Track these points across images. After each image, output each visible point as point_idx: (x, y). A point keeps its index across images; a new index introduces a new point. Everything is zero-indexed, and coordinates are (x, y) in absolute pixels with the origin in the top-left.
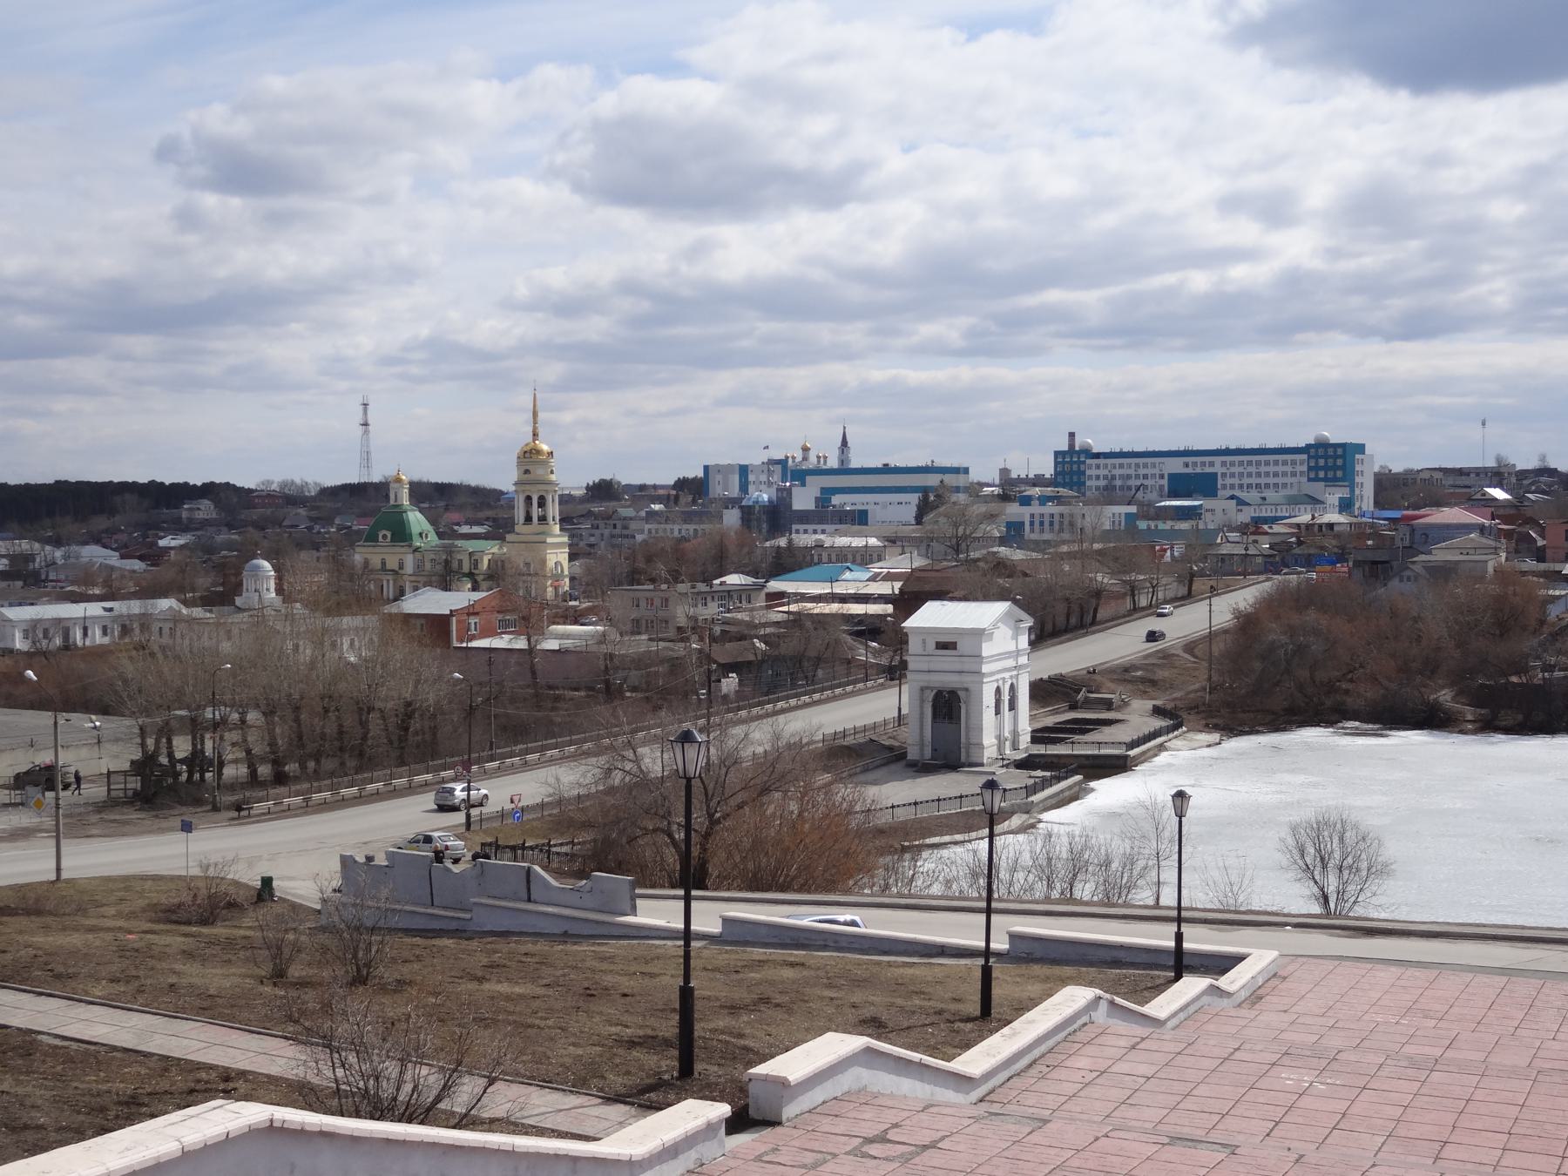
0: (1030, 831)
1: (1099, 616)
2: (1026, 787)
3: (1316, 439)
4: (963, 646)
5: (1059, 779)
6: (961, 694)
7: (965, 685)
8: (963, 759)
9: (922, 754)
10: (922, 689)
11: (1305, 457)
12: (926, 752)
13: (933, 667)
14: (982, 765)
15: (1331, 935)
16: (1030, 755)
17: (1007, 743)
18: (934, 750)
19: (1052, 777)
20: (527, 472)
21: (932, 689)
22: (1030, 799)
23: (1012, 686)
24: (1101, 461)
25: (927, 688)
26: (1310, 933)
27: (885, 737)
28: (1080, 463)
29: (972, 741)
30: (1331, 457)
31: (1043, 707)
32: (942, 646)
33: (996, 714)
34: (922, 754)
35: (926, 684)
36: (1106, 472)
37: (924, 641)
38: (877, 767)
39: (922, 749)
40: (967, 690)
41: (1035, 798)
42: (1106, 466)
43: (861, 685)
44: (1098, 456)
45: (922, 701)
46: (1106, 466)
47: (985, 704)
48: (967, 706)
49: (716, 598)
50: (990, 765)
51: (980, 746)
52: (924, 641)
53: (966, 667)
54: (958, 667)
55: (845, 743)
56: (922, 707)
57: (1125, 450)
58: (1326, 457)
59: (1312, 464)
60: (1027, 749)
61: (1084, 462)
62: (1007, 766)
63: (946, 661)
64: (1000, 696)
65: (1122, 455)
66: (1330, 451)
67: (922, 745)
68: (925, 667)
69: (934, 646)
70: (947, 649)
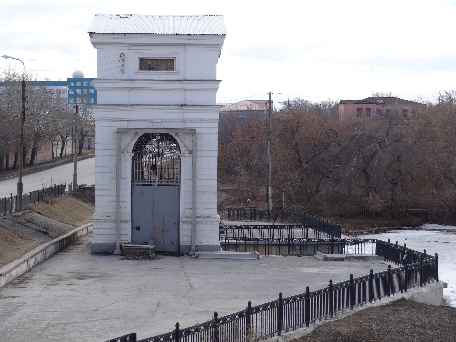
1: (39, 158)
3: (74, 75)
7: (189, 125)
11: (66, 88)
12: (123, 232)
13: (136, 98)
18: (136, 228)
25: (129, 130)
30: (85, 88)
35: (124, 125)
37: (122, 57)
39: (118, 229)
40: (193, 131)
45: (120, 152)
52: (122, 57)
56: (119, 161)
58: (82, 88)
59: (72, 93)
66: (85, 84)
69: (137, 65)
70: (157, 69)
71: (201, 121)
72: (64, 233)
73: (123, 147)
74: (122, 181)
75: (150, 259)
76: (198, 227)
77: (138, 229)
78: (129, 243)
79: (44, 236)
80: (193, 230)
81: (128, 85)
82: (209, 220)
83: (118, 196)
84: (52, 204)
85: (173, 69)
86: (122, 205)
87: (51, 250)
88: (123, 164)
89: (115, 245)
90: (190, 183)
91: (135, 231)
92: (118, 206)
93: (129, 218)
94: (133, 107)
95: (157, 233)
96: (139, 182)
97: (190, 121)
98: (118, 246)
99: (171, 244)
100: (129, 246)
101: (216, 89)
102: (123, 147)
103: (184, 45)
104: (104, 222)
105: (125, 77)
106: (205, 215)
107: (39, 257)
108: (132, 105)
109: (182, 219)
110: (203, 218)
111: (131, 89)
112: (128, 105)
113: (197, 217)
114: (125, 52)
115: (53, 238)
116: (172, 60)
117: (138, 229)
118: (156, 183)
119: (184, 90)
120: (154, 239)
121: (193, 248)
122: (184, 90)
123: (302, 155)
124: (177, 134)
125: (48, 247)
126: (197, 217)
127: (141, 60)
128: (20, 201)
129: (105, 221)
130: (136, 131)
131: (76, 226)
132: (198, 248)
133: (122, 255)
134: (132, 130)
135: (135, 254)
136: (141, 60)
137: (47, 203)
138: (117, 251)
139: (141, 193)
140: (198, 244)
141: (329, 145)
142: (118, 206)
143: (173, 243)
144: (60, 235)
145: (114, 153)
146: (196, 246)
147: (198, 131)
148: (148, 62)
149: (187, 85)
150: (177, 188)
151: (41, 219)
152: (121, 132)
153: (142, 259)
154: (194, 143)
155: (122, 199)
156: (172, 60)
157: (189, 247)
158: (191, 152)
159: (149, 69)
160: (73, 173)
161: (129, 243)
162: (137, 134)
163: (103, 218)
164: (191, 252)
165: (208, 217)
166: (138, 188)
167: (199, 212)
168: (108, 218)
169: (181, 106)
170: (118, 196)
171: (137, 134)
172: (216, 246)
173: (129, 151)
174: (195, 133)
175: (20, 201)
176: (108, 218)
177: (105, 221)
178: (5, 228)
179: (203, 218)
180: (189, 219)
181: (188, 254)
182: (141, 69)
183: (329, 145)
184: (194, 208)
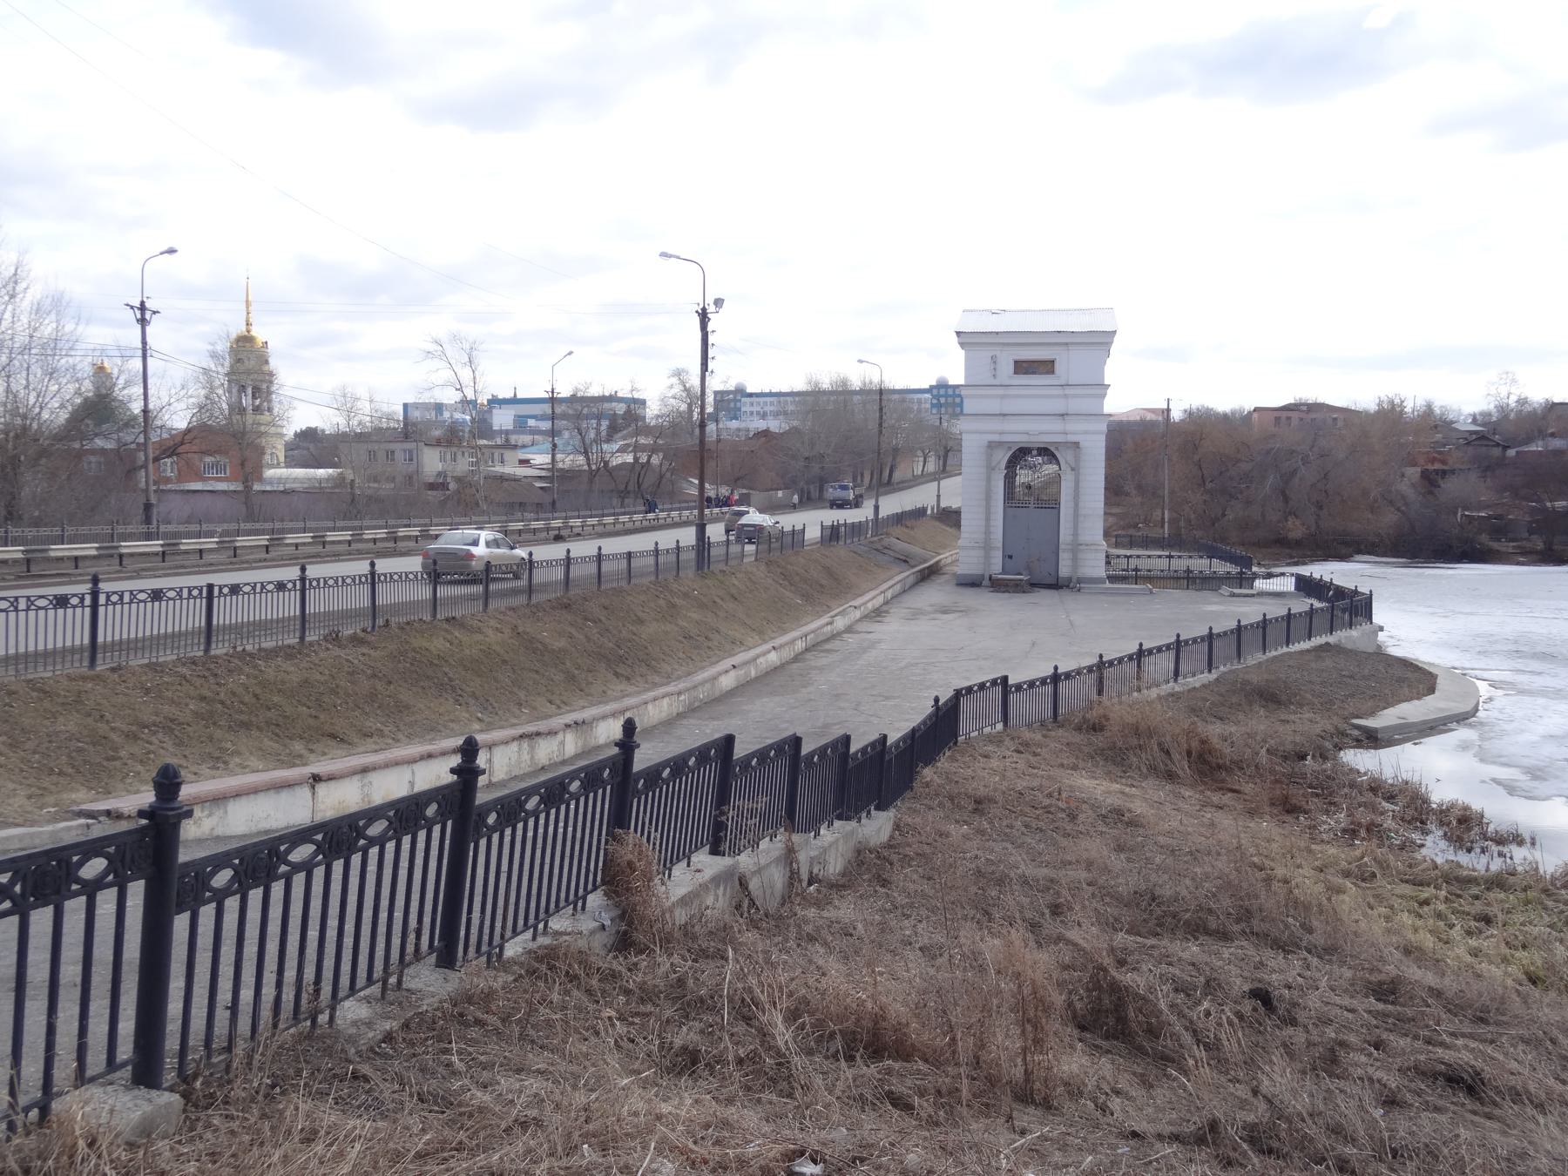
1: (897, 476)
4: (1070, 366)
7: (1071, 438)
11: (928, 396)
20: (239, 360)
24: (754, 399)
25: (1000, 444)
28: (735, 400)
30: (950, 396)
32: (1022, 367)
35: (996, 438)
36: (759, 409)
37: (994, 360)
39: (987, 557)
40: (1076, 445)
42: (759, 403)
44: (751, 395)
45: (990, 469)
46: (759, 403)
49: (466, 454)
52: (994, 360)
53: (1075, 405)
54: (1058, 406)
56: (989, 480)
57: (783, 391)
58: (946, 396)
59: (935, 401)
61: (740, 401)
63: (1035, 396)
65: (771, 394)
66: (950, 392)
67: (987, 547)
68: (993, 406)
70: (1034, 373)
71: (1086, 432)
72: (925, 561)
73: (993, 464)
75: (1024, 592)
76: (1081, 555)
77: (1010, 557)
79: (903, 564)
80: (1075, 559)
81: (1000, 391)
82: (1092, 547)
83: (988, 520)
84: (912, 528)
85: (1053, 372)
86: (992, 529)
87: (911, 580)
89: (983, 575)
90: (1072, 504)
92: (988, 532)
93: (1000, 545)
94: (1007, 417)
98: (987, 577)
100: (1000, 576)
101: (1104, 396)
102: (993, 464)
103: (1067, 344)
105: (997, 382)
107: (898, 588)
108: (1005, 415)
109: (1062, 547)
110: (1087, 545)
111: (1003, 397)
112: (1000, 415)
114: (998, 354)
115: (913, 567)
116: (1053, 362)
117: (1010, 557)
119: (1066, 396)
121: (1074, 580)
122: (1066, 396)
123: (1205, 472)
124: (1057, 449)
125: (908, 576)
127: (1016, 362)
128: (877, 525)
131: (939, 554)
132: (1080, 581)
133: (992, 587)
135: (1007, 585)
136: (1016, 362)
137: (907, 527)
138: (986, 582)
141: (1239, 460)
142: (988, 532)
144: (921, 563)
147: (1081, 445)
148: (1024, 365)
149: (1069, 391)
150: (1056, 511)
151: (900, 545)
152: (992, 446)
153: (1014, 592)
154: (1077, 458)
155: (992, 523)
156: (1053, 362)
157: (1070, 579)
158: (1073, 469)
159: (1025, 373)
162: (1010, 448)
164: (1071, 585)
166: (1009, 510)
167: (1082, 539)
169: (1063, 415)
170: (988, 520)
171: (1010, 448)
174: (1078, 448)
175: (877, 525)
178: (860, 555)
179: (1087, 545)
180: (1070, 547)
181: (1068, 586)
182: (1015, 373)
183: (1239, 460)
184: (1075, 534)
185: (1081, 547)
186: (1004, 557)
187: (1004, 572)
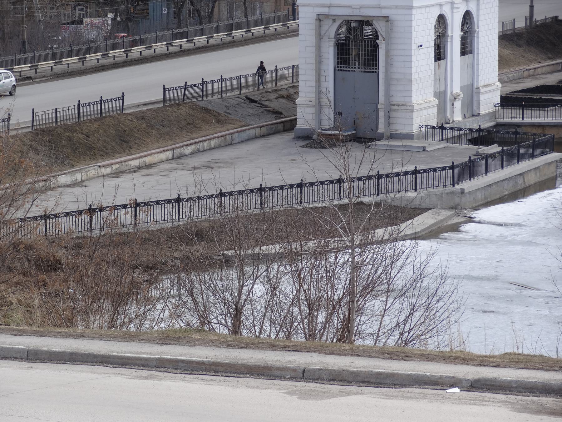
0: (442, 236)
2: (452, 167)
5: (518, 158)
6: (380, 26)
7: (384, 12)
8: (382, 128)
9: (320, 121)
10: (320, 19)
12: (324, 117)
14: (410, 137)
15: (526, 409)
16: (498, 125)
17: (458, 104)
18: (338, 113)
19: (502, 152)
21: (333, 18)
22: (458, 187)
23: (467, 16)
25: (327, 16)
26: (482, 402)
27: (272, 96)
29: (396, 99)
31: (550, 58)
33: (436, 60)
34: (320, 121)
35: (325, 11)
38: (249, 140)
40: (386, 19)
41: (467, 185)
43: (277, 26)
45: (320, 37)
47: (415, 42)
48: (387, 45)
50: (423, 137)
51: (408, 109)
55: (202, 104)
56: (319, 48)
60: (493, 115)
62: (457, 139)
64: (445, 27)
67: (319, 106)
74: (324, 67)
76: (393, 114)
77: (341, 114)
78: (329, 129)
82: (403, 107)
88: (324, 50)
91: (337, 117)
95: (358, 119)
96: (341, 67)
97: (385, 8)
99: (371, 131)
102: (322, 33)
104: (307, 107)
106: (401, 103)
109: (379, 106)
110: (398, 106)
113: (393, 105)
118: (357, 69)
120: (355, 126)
126: (393, 105)
129: (308, 106)
130: (333, 18)
134: (330, 17)
139: (343, 79)
140: (393, 132)
143: (372, 130)
145: (313, 38)
146: (390, 134)
147: (392, 17)
150: (376, 74)
160: (529, 4)
161: (329, 129)
163: (305, 103)
165: (403, 105)
168: (310, 103)
172: (410, 134)
173: (330, 37)
176: (310, 103)
177: (308, 106)
179: (398, 106)
185: (395, 107)
186: (335, 113)
187: (335, 128)
